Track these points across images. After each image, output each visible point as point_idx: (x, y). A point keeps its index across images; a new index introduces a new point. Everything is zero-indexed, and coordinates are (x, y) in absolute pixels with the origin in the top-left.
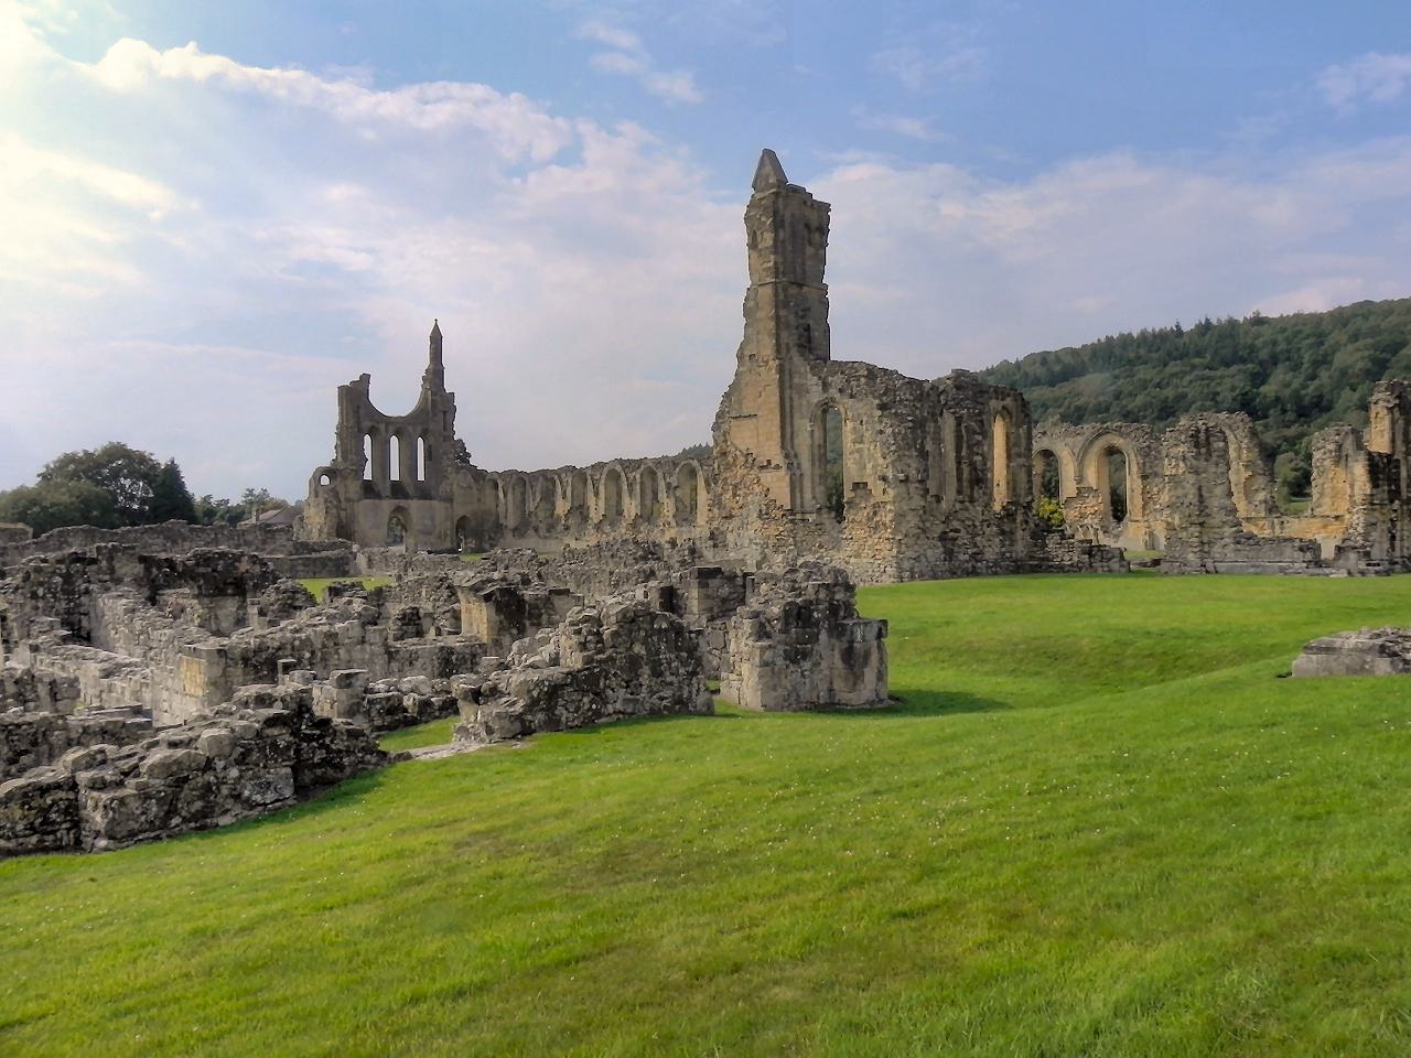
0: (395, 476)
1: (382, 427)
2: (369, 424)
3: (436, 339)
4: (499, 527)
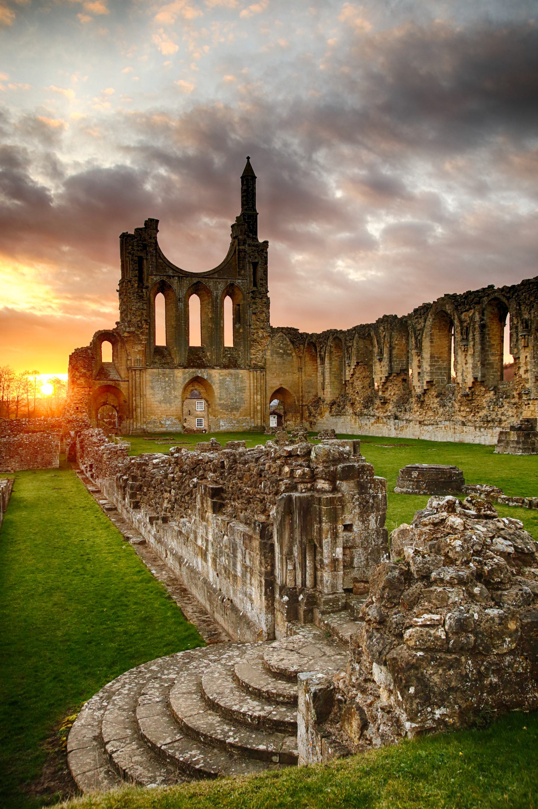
0: (195, 339)
1: (175, 283)
2: (156, 279)
3: (249, 179)
4: (318, 401)
